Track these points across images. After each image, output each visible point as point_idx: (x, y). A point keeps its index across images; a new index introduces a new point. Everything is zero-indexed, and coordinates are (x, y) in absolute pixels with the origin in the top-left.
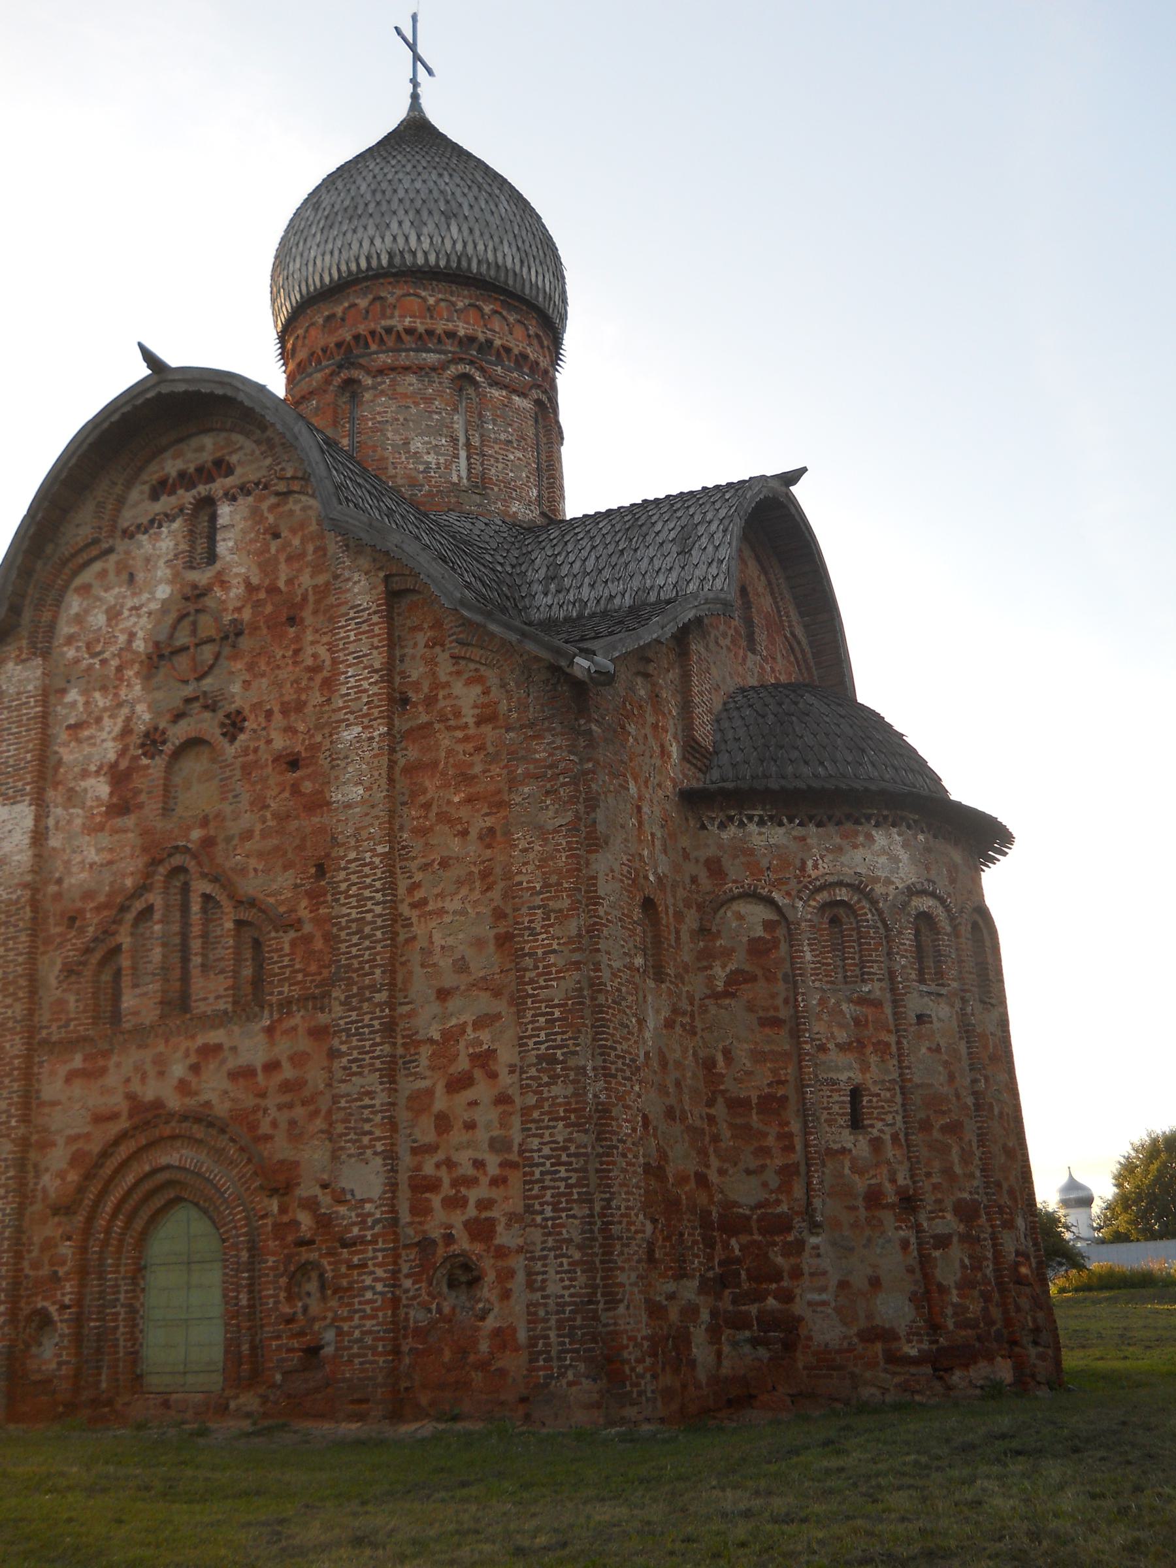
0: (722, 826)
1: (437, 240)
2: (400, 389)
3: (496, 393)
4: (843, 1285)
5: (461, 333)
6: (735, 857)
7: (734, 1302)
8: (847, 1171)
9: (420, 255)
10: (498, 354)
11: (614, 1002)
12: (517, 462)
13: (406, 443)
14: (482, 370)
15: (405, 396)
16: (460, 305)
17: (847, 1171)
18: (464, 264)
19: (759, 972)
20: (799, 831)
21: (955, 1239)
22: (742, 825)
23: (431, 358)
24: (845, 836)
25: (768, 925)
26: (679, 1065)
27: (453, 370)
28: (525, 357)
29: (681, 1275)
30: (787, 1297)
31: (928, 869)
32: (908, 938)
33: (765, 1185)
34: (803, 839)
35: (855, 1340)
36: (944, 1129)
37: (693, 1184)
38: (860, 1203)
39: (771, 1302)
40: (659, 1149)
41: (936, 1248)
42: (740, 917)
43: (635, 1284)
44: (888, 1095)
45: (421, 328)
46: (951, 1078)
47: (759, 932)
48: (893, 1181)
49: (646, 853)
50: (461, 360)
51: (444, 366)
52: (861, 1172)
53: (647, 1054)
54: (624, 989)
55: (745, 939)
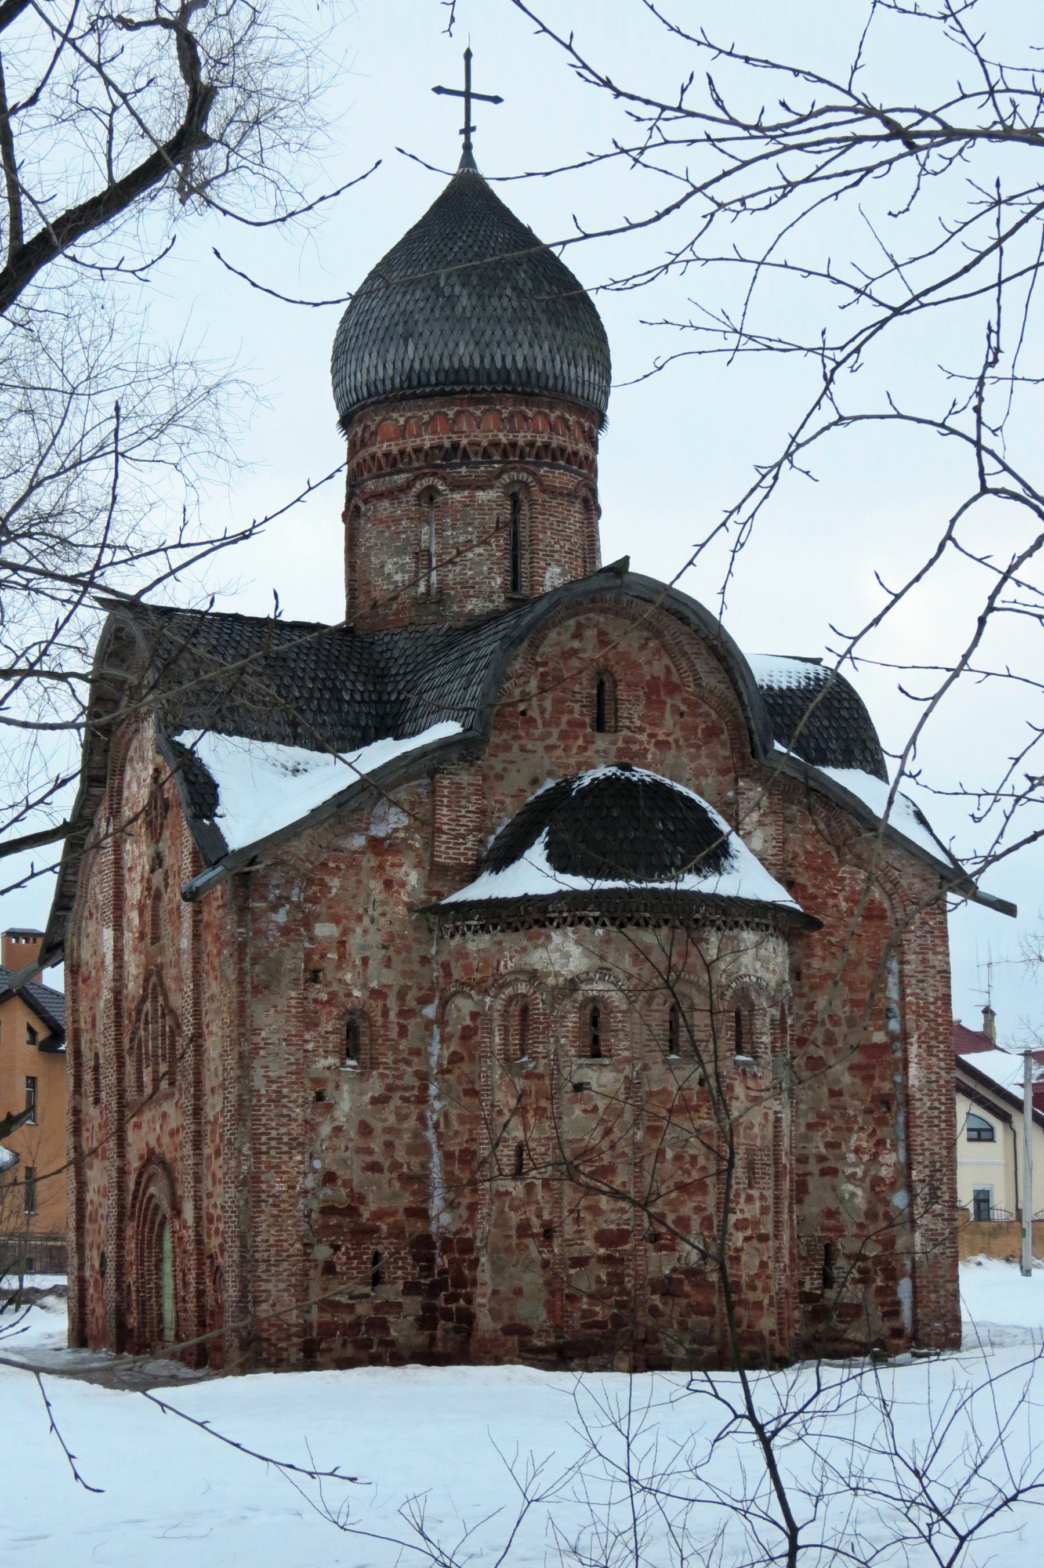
0: (452, 936)
1: (399, 364)
2: (379, 516)
3: (457, 496)
4: (495, 1292)
5: (427, 445)
6: (457, 960)
7: (446, 1301)
8: (506, 1209)
9: (388, 382)
10: (465, 455)
11: (269, 1101)
12: (477, 559)
13: (383, 566)
14: (444, 479)
15: (381, 522)
16: (426, 417)
17: (506, 1209)
18: (424, 379)
19: (465, 1054)
20: (500, 936)
21: (593, 1261)
22: (464, 934)
23: (401, 479)
24: (530, 939)
25: (474, 1016)
26: (388, 1130)
27: (418, 486)
28: (495, 444)
29: (376, 1280)
30: (469, 1300)
31: (602, 958)
32: (572, 1020)
33: (460, 1217)
34: (500, 943)
35: (500, 1333)
36: (591, 1175)
37: (401, 1216)
38: (513, 1232)
39: (462, 1302)
40: (351, 1194)
41: (573, 1267)
42: (459, 1010)
43: (284, 1290)
44: (543, 1149)
45: (395, 450)
46: (608, 1132)
47: (468, 1022)
48: (539, 1216)
49: (348, 977)
50: (425, 475)
51: (409, 485)
52: (514, 1208)
53: (337, 1130)
54: (285, 1091)
55: (459, 1027)
